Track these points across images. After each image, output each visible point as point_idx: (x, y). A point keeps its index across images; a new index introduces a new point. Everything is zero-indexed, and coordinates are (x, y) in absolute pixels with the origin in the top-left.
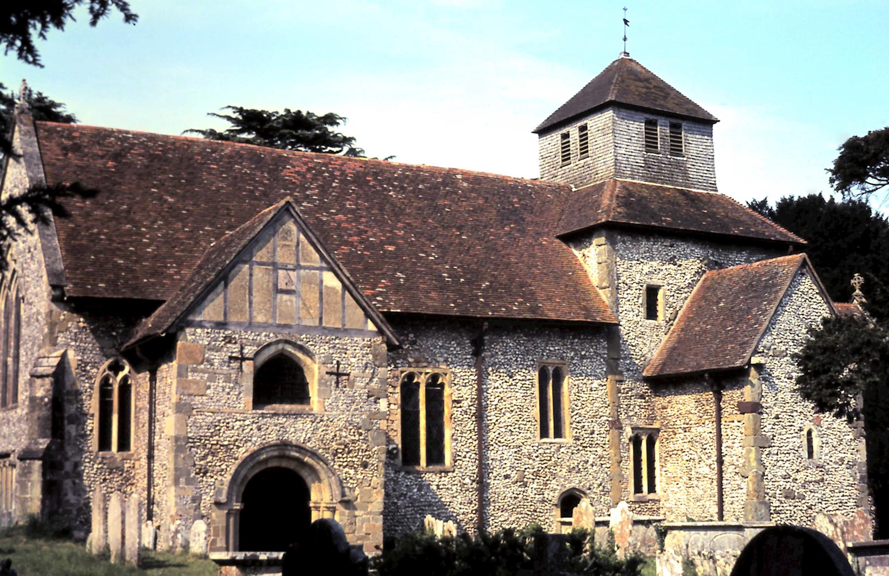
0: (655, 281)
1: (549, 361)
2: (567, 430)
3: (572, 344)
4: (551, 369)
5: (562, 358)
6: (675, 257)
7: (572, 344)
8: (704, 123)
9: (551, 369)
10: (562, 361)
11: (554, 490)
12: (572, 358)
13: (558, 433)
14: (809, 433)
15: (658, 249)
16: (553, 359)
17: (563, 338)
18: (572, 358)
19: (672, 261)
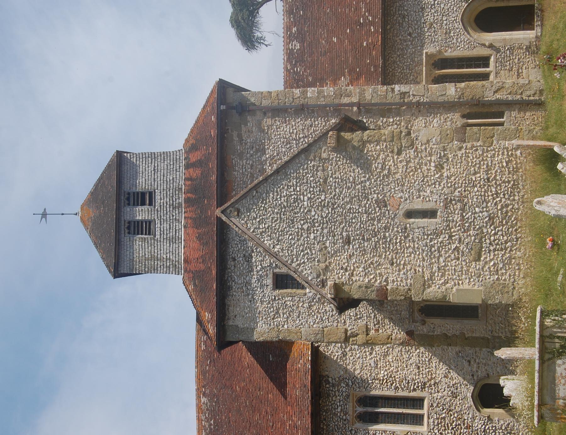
0: (269, 281)
1: (351, 413)
2: (417, 394)
3: (333, 386)
4: (360, 409)
5: (348, 396)
6: (244, 255)
7: (333, 386)
8: (121, 163)
9: (360, 409)
10: (351, 397)
11: (474, 418)
12: (347, 385)
13: (418, 402)
14: (410, 214)
15: (238, 276)
16: (350, 407)
17: (329, 395)
18: (347, 385)
19: (248, 258)
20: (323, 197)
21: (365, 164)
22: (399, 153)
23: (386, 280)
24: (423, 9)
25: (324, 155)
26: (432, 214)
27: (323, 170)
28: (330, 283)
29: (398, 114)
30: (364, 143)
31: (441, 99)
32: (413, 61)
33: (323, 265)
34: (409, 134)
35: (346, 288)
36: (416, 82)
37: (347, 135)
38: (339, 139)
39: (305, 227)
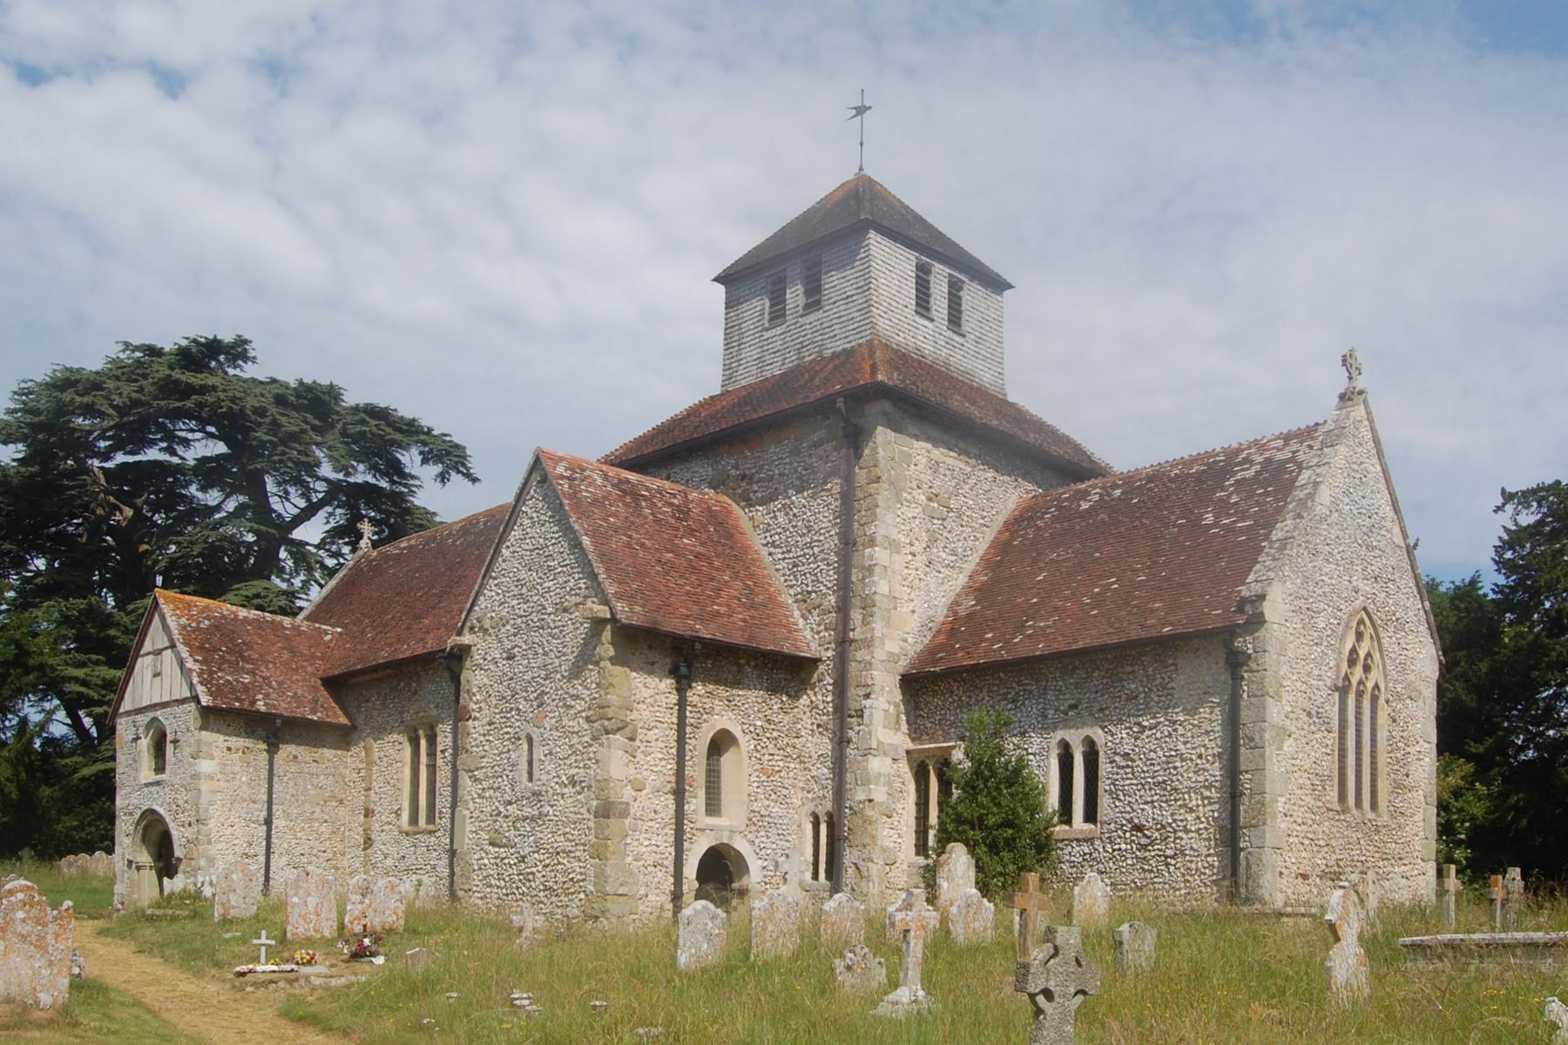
20: (550, 610)
21: (576, 672)
22: (588, 719)
23: (475, 719)
24: (1023, 734)
25: (589, 604)
26: (531, 779)
27: (577, 605)
28: (467, 639)
29: (836, 709)
30: (597, 663)
31: (849, 777)
32: (951, 726)
33: (487, 623)
34: (607, 733)
35: (468, 663)
36: (916, 733)
37: (607, 634)
38: (603, 621)
39: (524, 591)
